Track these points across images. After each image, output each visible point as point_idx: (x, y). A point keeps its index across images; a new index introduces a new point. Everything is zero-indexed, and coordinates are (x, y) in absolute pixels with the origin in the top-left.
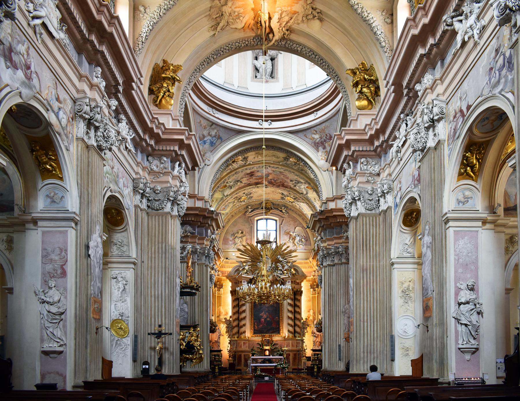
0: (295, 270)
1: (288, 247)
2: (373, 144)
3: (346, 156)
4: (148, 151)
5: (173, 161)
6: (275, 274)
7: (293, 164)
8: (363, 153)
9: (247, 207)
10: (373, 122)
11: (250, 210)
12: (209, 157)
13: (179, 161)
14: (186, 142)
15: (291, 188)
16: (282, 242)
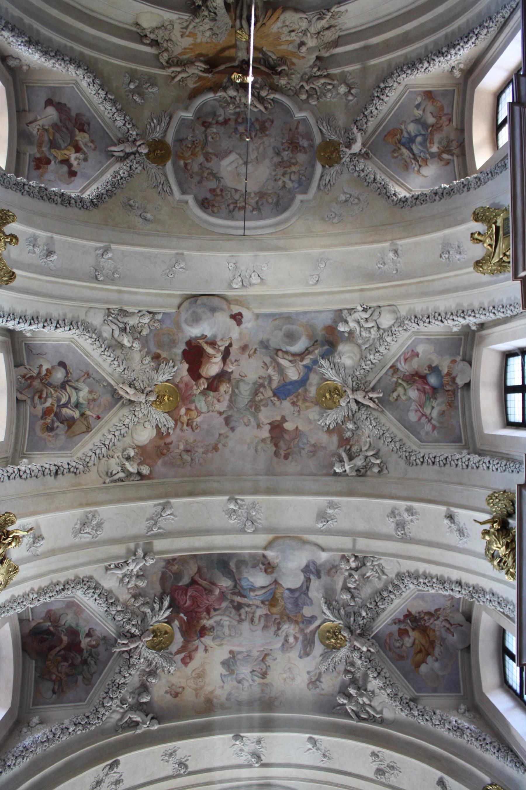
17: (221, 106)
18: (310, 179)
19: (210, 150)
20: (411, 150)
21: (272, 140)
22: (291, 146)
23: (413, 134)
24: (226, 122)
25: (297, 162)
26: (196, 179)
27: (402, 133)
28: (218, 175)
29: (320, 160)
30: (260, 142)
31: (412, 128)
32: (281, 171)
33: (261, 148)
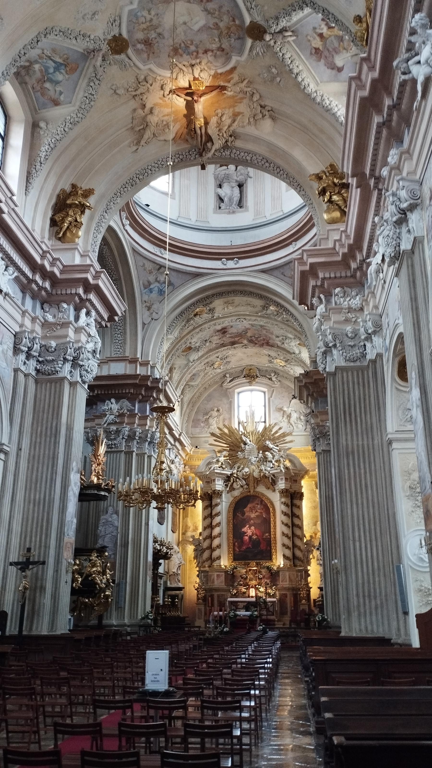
0: (290, 461)
1: (280, 429)
2: (350, 268)
3: (314, 287)
4: (42, 296)
5: (77, 309)
6: (263, 467)
7: (275, 313)
8: (337, 281)
9: (225, 376)
10: (343, 235)
12: (158, 310)
13: (87, 308)
14: (91, 281)
15: (278, 347)
16: (273, 422)
18: (130, 21)
19: (216, 31)
20: (55, 62)
23: (57, 73)
24: (206, 52)
26: (224, 9)
27: (66, 72)
28: (205, 12)
29: (124, 39)
31: (59, 77)
32: (155, 22)
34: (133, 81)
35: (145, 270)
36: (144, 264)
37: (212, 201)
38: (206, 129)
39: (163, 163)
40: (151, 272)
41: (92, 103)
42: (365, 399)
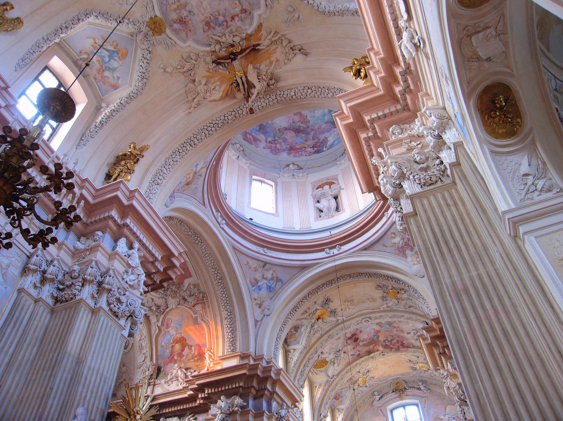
8: (388, 120)
9: (374, 395)
11: (378, 397)
15: (414, 347)
17: (241, 28)
20: (107, 50)
21: (198, 19)
22: (184, 20)
23: (112, 60)
24: (233, 19)
25: (175, 11)
27: (119, 58)
29: (160, 18)
30: (205, 15)
31: (114, 64)
33: (202, 10)
34: (179, 59)
35: (250, 267)
36: (248, 262)
37: (312, 212)
38: (246, 77)
39: (217, 122)
40: (256, 270)
41: (145, 80)
42: (463, 220)
